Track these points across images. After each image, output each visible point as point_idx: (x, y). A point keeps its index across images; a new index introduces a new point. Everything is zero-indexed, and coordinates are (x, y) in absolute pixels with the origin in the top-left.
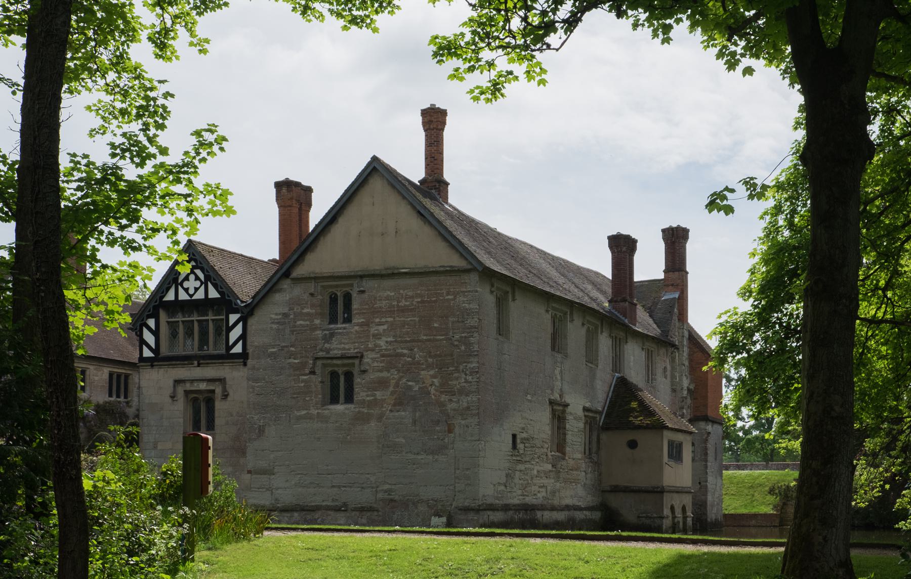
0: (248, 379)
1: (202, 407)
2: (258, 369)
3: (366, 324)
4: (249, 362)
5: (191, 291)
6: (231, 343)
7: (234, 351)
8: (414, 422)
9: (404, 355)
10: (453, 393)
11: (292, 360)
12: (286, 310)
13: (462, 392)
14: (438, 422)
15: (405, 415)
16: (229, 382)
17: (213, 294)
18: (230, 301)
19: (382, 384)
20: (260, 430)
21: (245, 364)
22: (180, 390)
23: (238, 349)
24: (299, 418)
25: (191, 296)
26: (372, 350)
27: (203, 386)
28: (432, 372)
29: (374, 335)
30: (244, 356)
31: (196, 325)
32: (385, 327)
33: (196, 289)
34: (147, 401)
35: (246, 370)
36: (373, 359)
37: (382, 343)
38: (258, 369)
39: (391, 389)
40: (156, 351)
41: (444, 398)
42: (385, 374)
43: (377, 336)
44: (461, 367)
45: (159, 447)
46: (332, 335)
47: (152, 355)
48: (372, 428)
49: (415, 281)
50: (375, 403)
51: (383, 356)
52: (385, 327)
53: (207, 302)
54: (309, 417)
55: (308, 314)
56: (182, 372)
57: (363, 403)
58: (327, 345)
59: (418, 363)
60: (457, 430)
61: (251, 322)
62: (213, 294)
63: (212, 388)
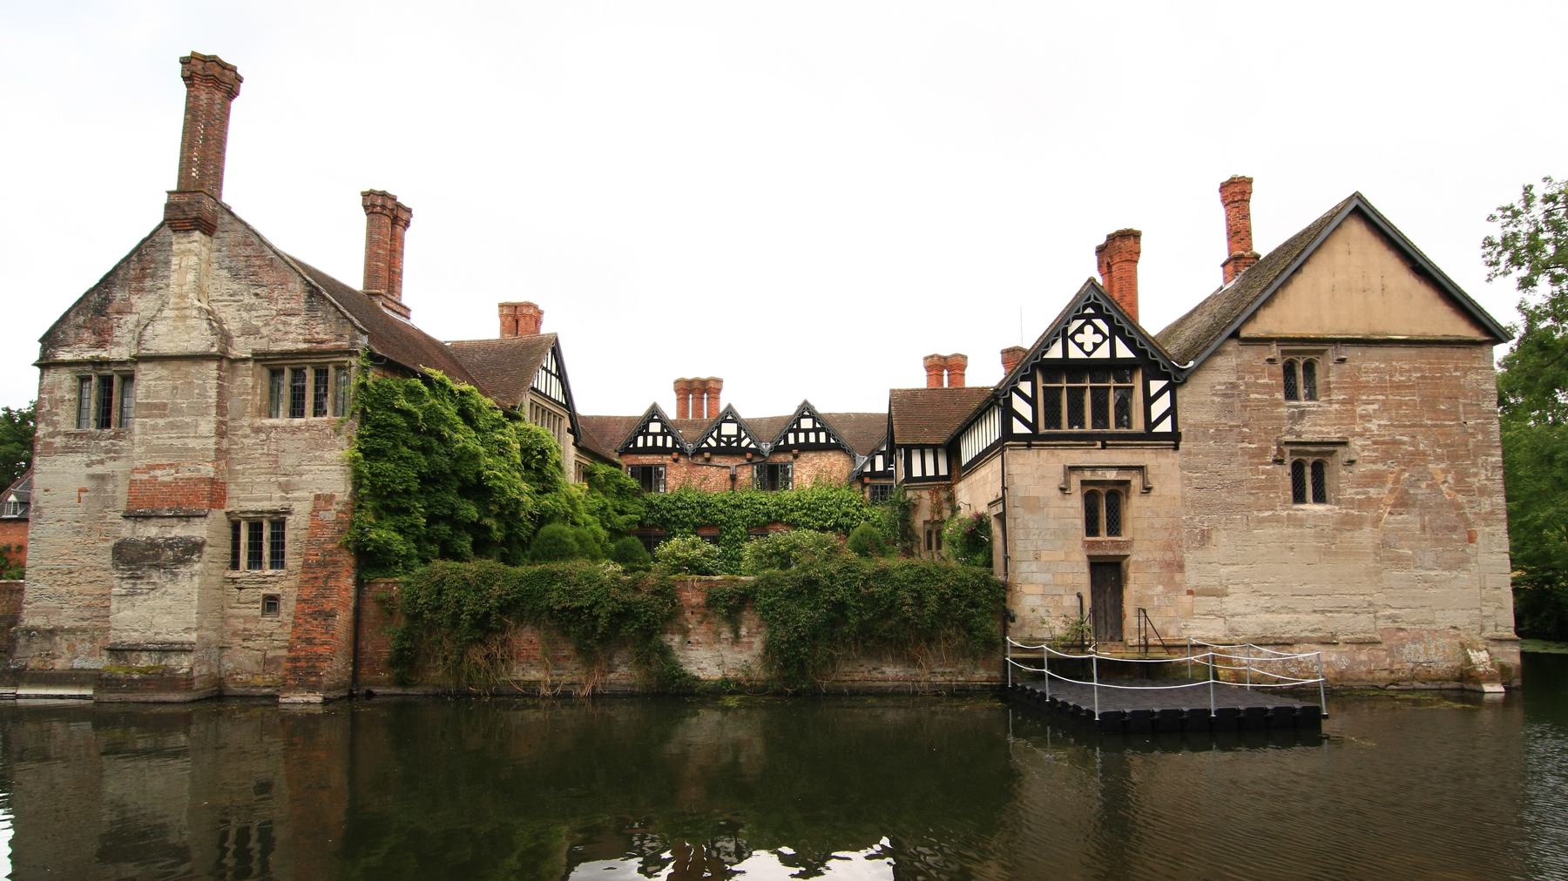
0: (1182, 468)
1: (1104, 504)
2: (1197, 454)
3: (1350, 401)
4: (1182, 444)
5: (1088, 348)
6: (1154, 418)
7: (1157, 430)
8: (1423, 528)
9: (1404, 443)
10: (1468, 491)
11: (1245, 445)
12: (1233, 379)
13: (1483, 491)
14: (1454, 529)
15: (1411, 520)
16: (1151, 471)
17: (1123, 352)
18: (1157, 363)
19: (1376, 479)
20: (1203, 536)
21: (1176, 448)
22: (1075, 480)
23: (1165, 426)
24: (1261, 521)
25: (1089, 354)
26: (1361, 435)
27: (1112, 475)
28: (1443, 466)
29: (1361, 417)
30: (1174, 437)
31: (1088, 392)
32: (1376, 406)
33: (1096, 346)
34: (1021, 494)
35: (1176, 454)
36: (1363, 448)
37: (1373, 426)
38: (1197, 454)
39: (1389, 485)
40: (1033, 426)
41: (1461, 498)
42: (1380, 467)
43: (1366, 418)
44: (1480, 461)
45: (1043, 558)
46: (1302, 414)
47: (1027, 431)
48: (1366, 536)
49: (1413, 352)
50: (1369, 502)
51: (1375, 443)
52: (1376, 406)
53: (1113, 366)
54: (1276, 520)
55: (1265, 386)
56: (1078, 457)
57: (1352, 501)
58: (1297, 428)
59: (1424, 453)
60: (1479, 538)
61: (1179, 393)
62: (1123, 352)
63: (1124, 478)
